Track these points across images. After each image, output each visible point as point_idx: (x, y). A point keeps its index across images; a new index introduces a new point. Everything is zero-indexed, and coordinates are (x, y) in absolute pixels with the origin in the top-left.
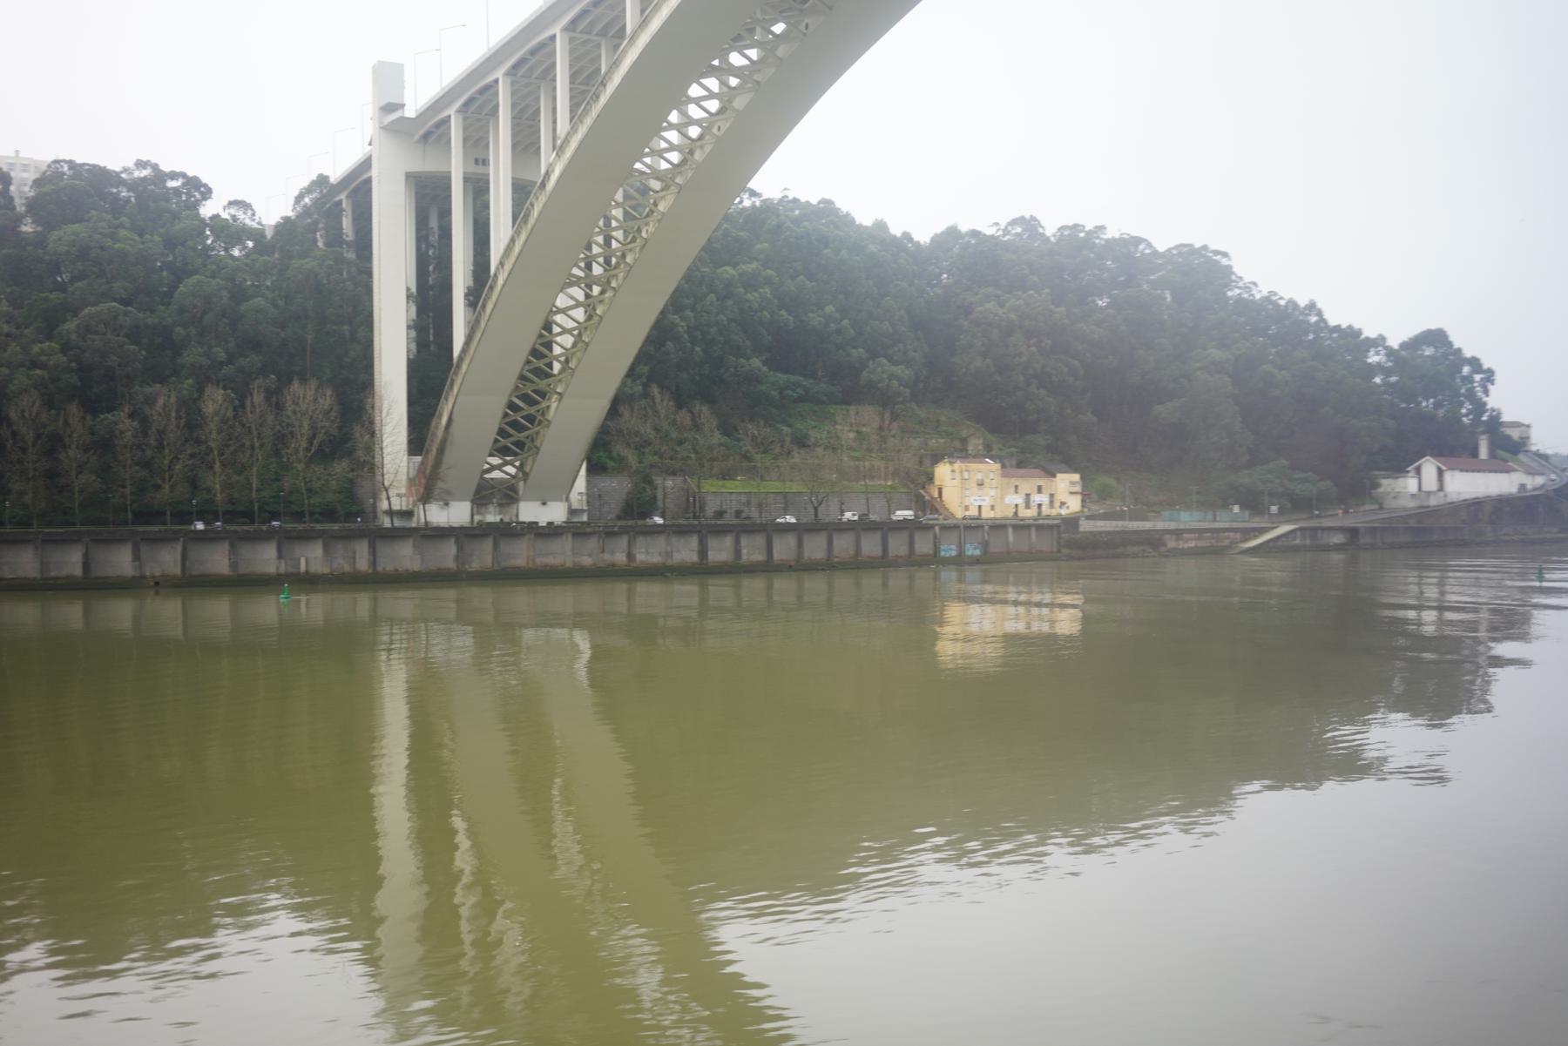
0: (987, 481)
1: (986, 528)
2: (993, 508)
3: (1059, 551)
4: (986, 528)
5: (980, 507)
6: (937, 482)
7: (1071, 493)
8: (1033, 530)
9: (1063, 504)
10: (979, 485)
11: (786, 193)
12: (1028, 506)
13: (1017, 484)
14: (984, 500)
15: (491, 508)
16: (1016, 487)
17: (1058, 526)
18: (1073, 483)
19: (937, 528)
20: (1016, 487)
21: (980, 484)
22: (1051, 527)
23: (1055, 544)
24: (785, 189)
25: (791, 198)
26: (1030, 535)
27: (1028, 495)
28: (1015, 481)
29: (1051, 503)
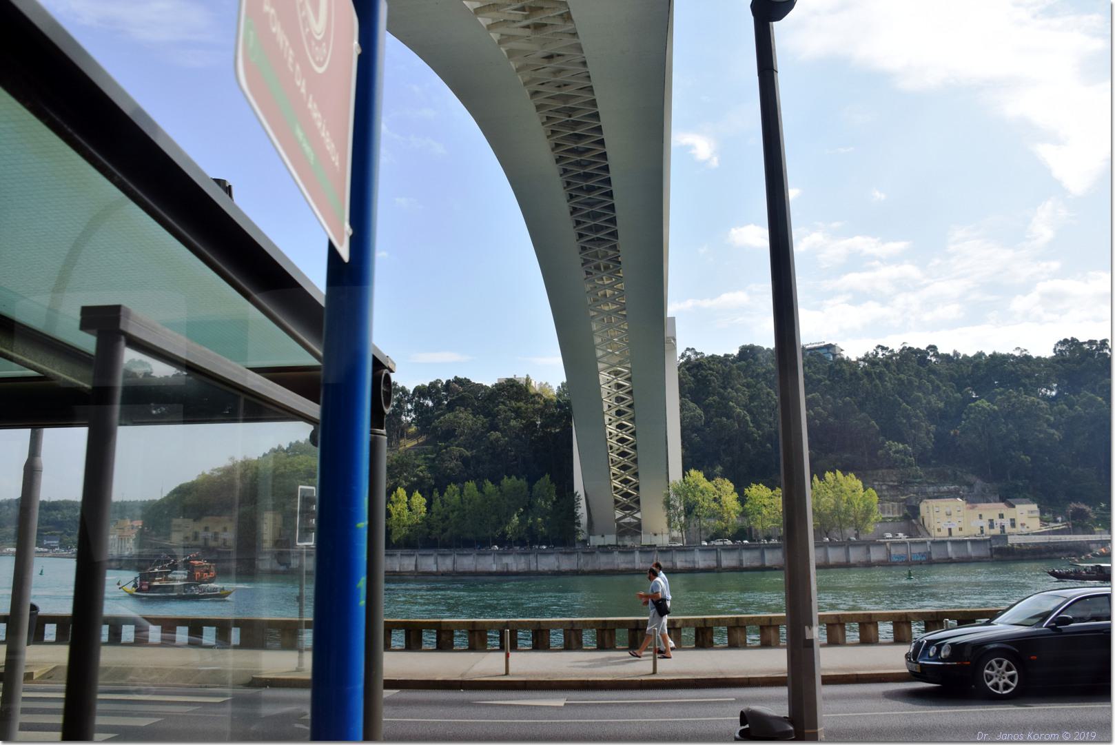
0: (954, 513)
1: (929, 543)
2: (961, 529)
3: (992, 556)
4: (929, 543)
5: (950, 530)
6: (922, 515)
7: (1029, 517)
8: (969, 544)
9: (1023, 525)
10: (947, 515)
11: (904, 345)
12: (992, 526)
13: (980, 513)
14: (952, 524)
15: (627, 538)
16: (981, 516)
17: (989, 540)
18: (1032, 512)
19: (888, 544)
20: (981, 516)
21: (949, 514)
22: (985, 541)
23: (989, 551)
24: (904, 343)
25: (908, 347)
26: (967, 546)
27: (991, 521)
28: (976, 512)
29: (1013, 525)
